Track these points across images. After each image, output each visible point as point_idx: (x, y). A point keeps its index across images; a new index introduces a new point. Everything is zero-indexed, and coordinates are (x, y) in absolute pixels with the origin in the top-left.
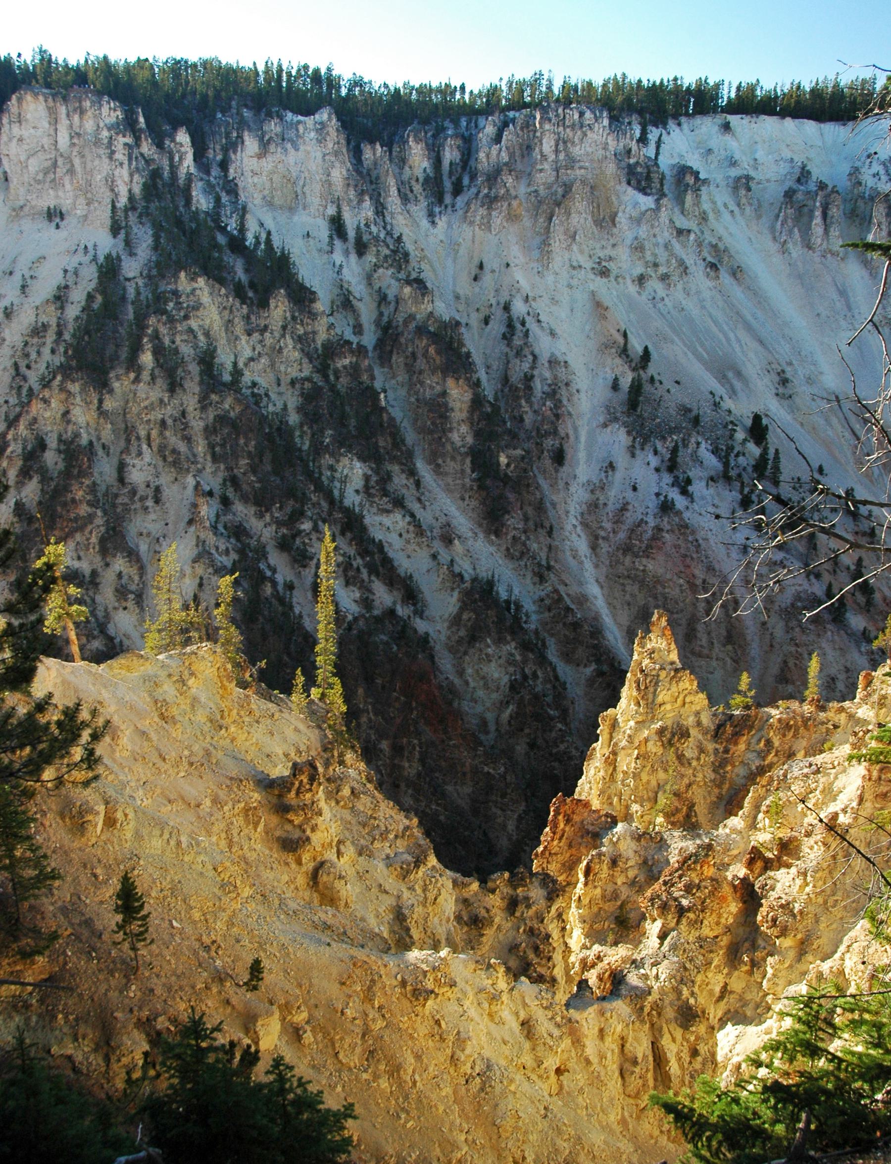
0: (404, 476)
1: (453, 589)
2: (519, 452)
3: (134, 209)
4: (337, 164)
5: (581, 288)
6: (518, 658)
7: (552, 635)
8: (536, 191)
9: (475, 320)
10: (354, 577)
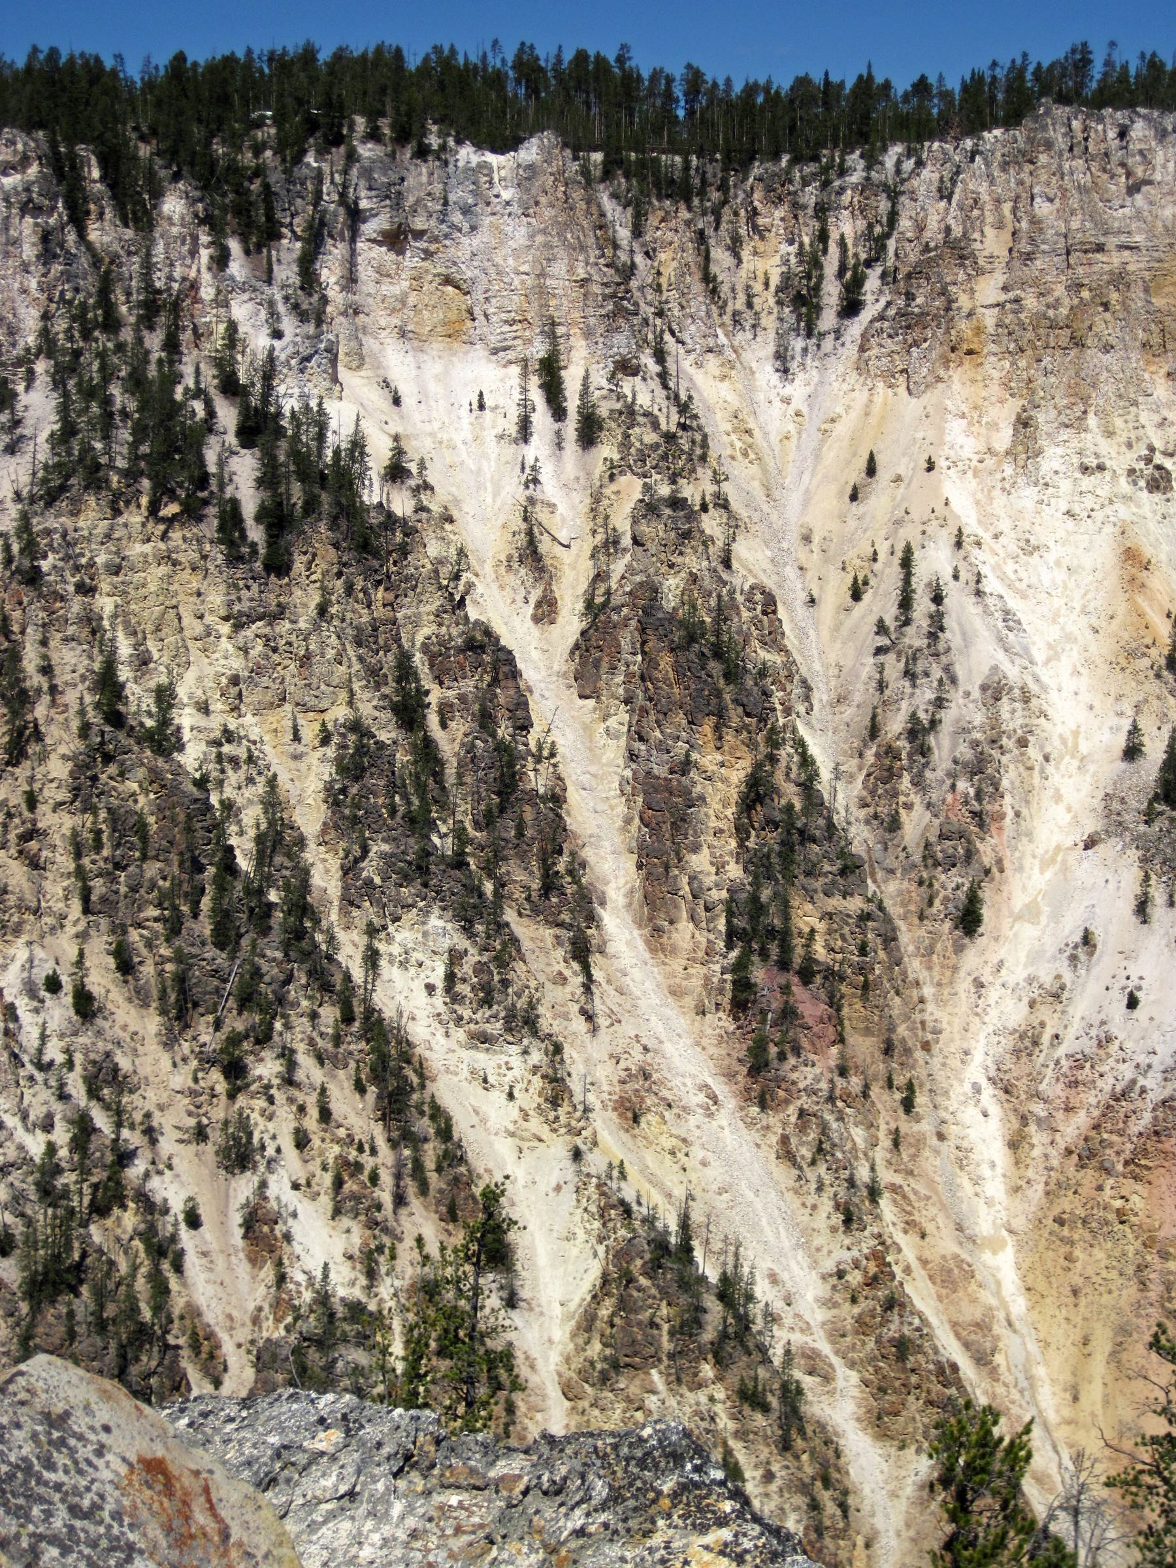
0: (560, 953)
1: (601, 1239)
2: (855, 904)
3: (49, 357)
4: (561, 253)
5: (1099, 516)
6: (725, 1423)
7: (852, 1365)
8: (1017, 300)
9: (835, 590)
10: (356, 1198)
